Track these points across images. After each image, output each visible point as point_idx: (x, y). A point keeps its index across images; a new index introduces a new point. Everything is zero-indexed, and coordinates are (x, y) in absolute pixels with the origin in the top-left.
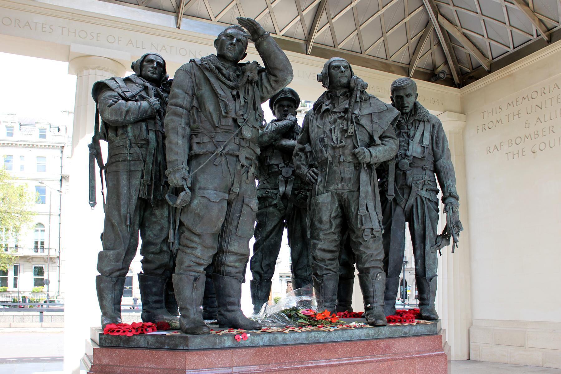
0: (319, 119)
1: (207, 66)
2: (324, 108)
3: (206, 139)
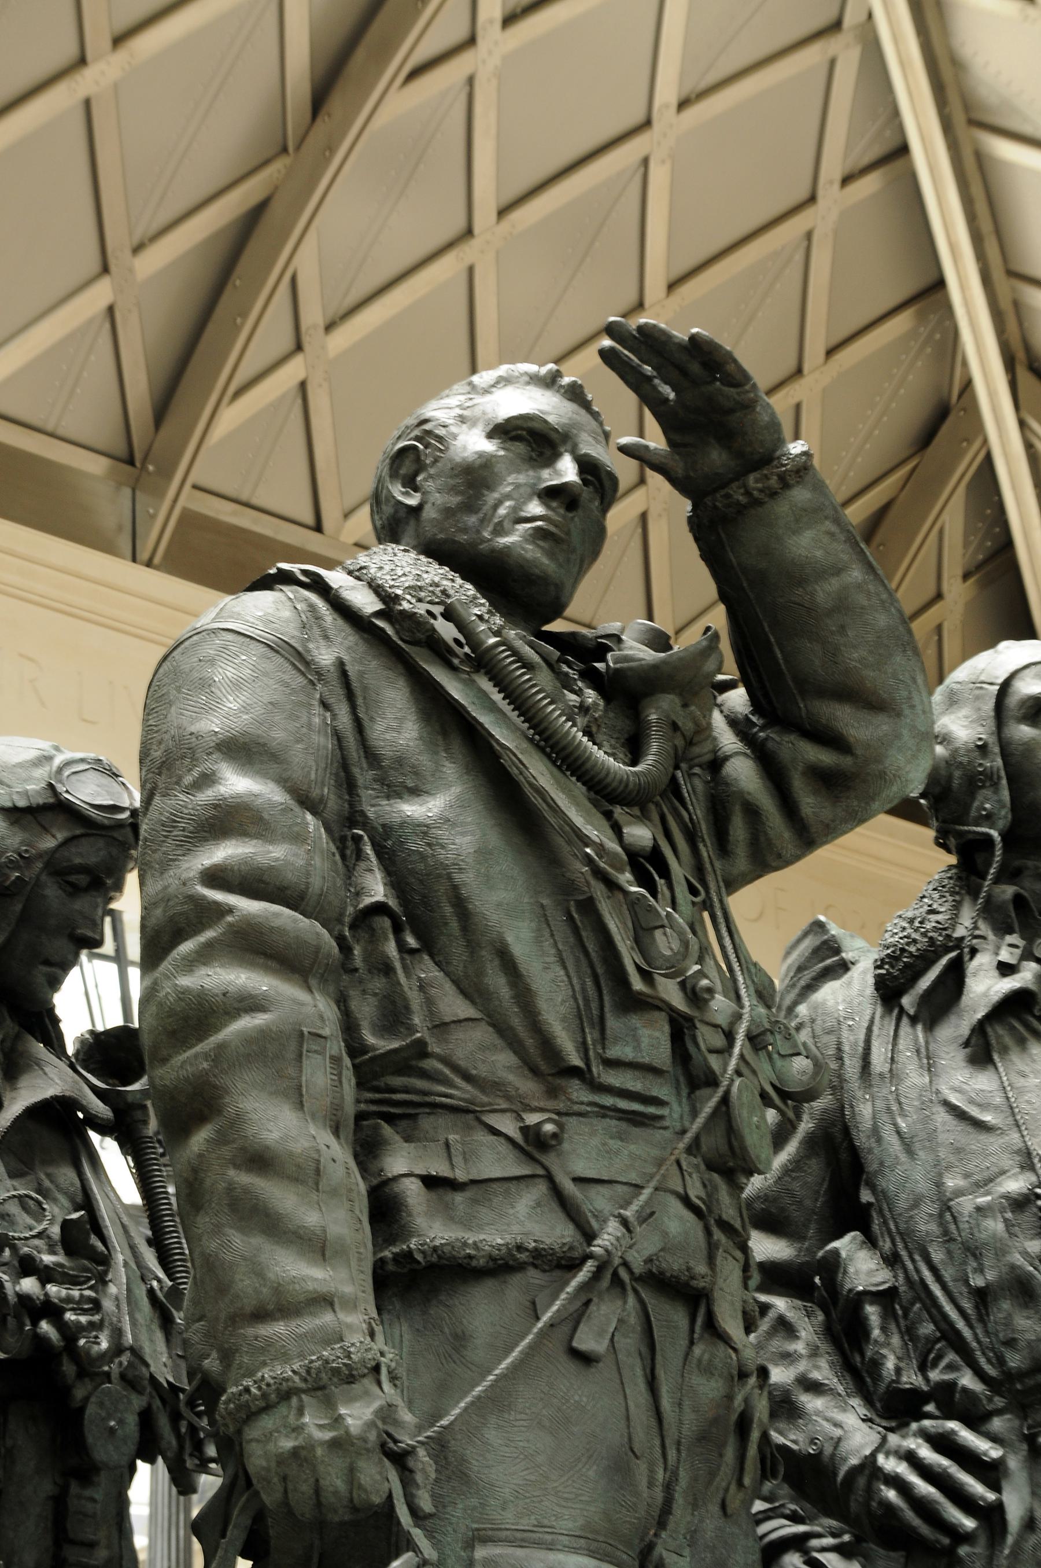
1: (447, 630)
3: (494, 1161)
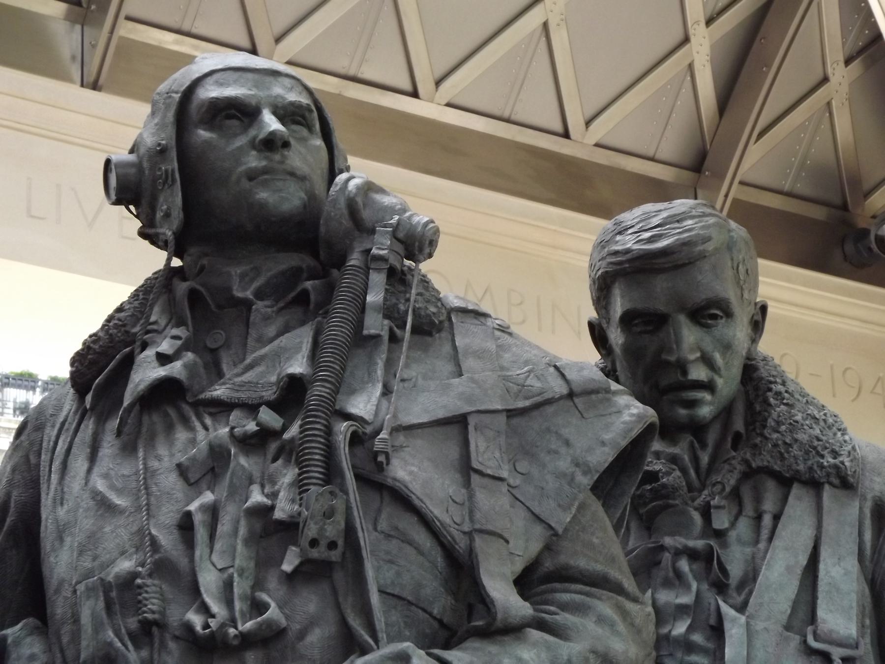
0: (109, 447)
2: (147, 372)
